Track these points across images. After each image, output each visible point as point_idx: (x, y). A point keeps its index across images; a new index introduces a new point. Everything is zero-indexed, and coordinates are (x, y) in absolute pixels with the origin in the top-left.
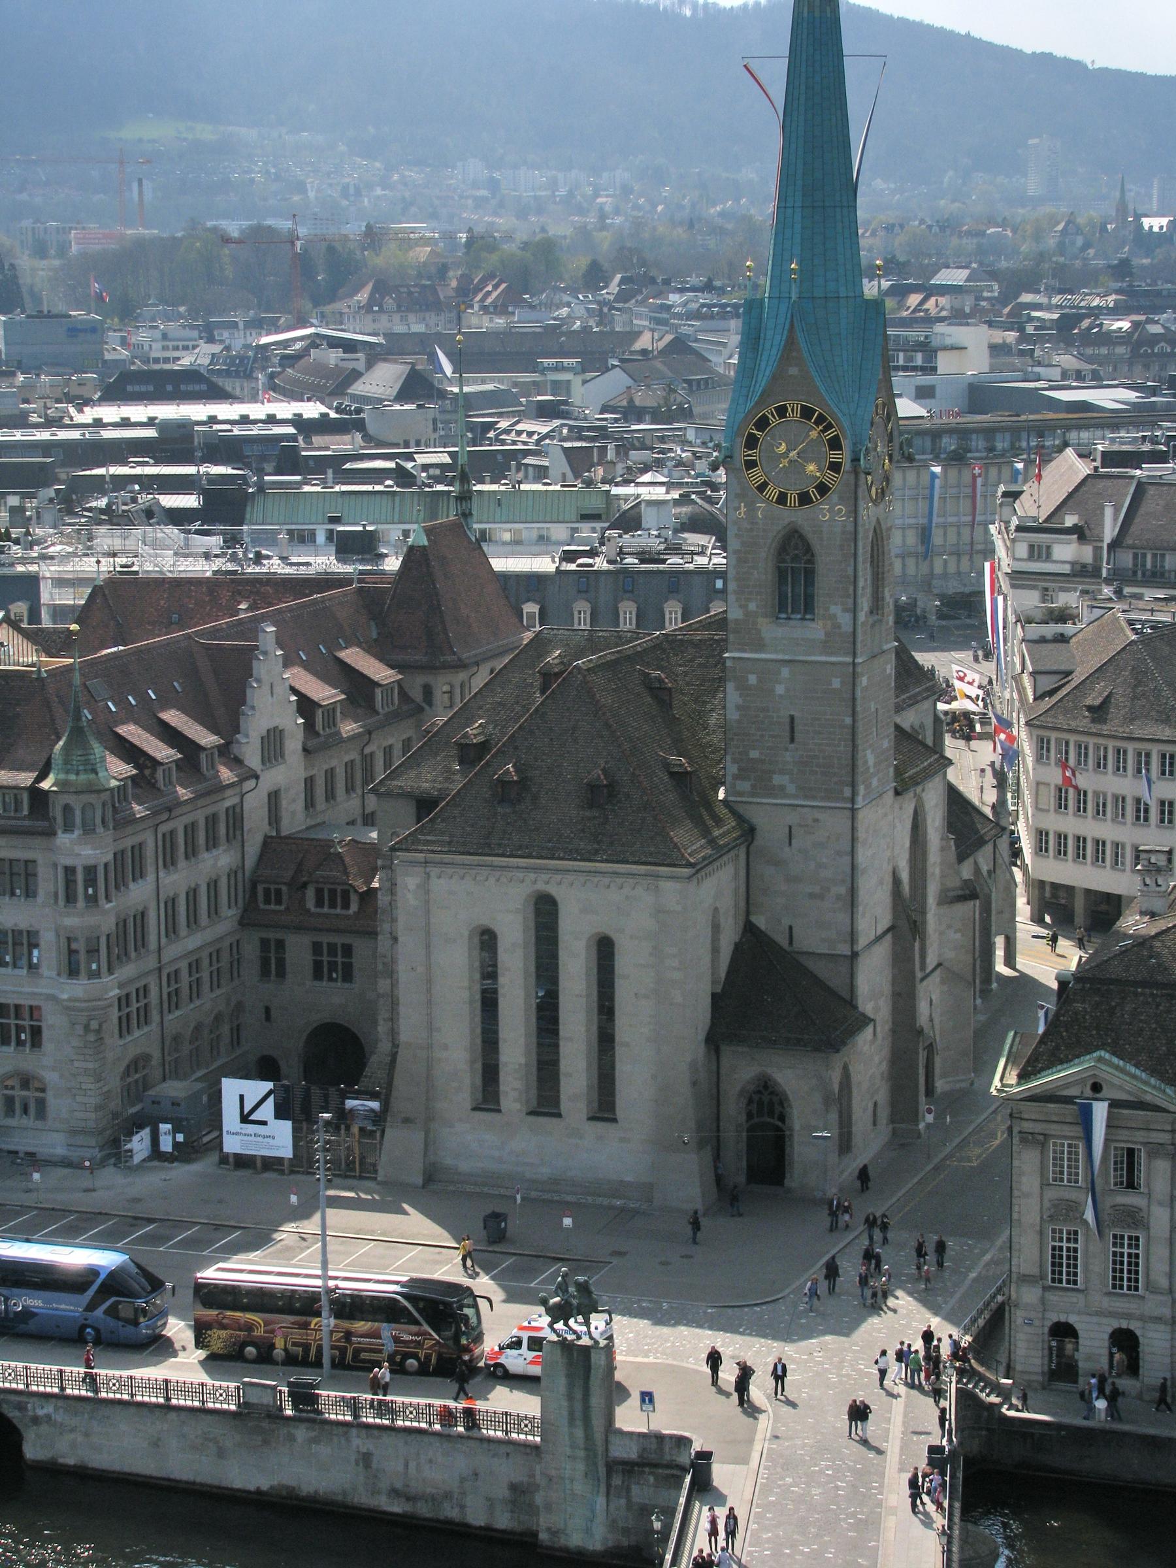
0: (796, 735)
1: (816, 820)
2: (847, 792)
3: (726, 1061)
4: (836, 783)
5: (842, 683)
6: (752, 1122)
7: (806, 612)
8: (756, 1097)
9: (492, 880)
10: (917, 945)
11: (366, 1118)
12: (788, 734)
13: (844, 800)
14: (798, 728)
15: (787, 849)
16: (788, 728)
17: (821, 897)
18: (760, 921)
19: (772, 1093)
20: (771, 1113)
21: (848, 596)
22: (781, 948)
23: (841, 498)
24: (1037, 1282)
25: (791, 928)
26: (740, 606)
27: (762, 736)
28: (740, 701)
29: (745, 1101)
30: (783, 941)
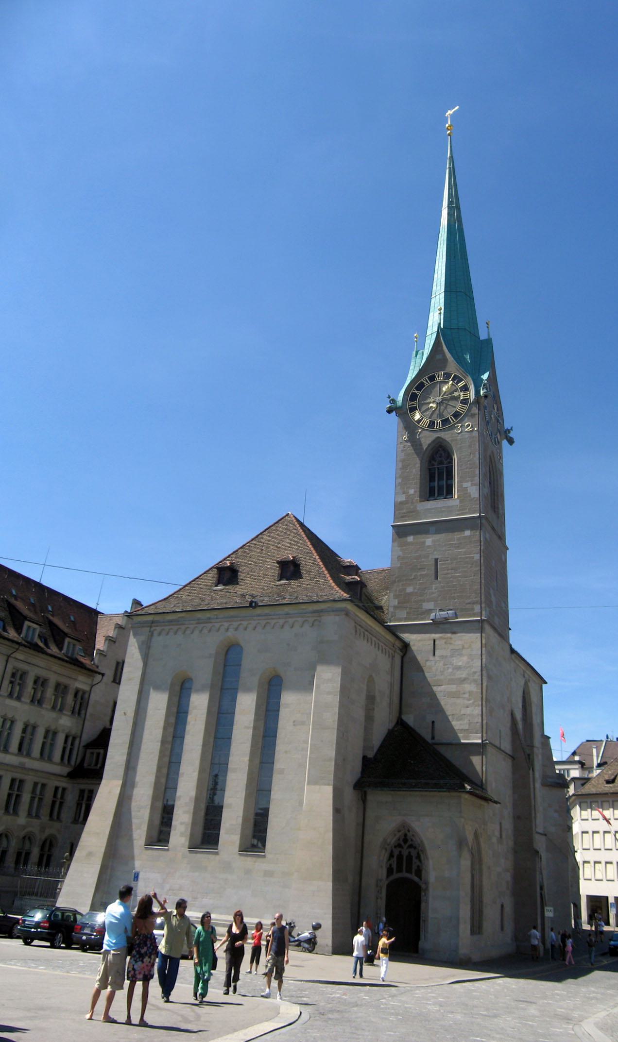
2: (477, 608)
3: (370, 813)
4: (469, 603)
6: (392, 878)
7: (446, 495)
8: (396, 853)
12: (433, 572)
13: (474, 615)
15: (432, 658)
16: (433, 568)
17: (455, 695)
18: (410, 719)
19: (411, 846)
20: (409, 870)
22: (424, 741)
25: (433, 722)
29: (387, 855)
30: (428, 737)
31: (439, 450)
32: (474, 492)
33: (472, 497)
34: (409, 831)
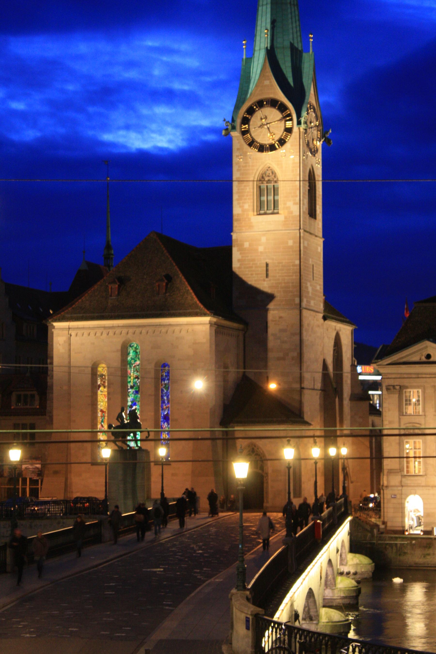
0: (270, 273)
1: (281, 317)
2: (297, 300)
5: (294, 243)
9: (105, 335)
10: (337, 400)
11: (33, 472)
12: (265, 272)
14: (270, 268)
16: (265, 269)
17: (283, 359)
21: (296, 196)
23: (292, 146)
24: (398, 472)
26: (240, 207)
27: (252, 274)
28: (240, 257)
31: (267, 170)
32: (295, 210)
33: (294, 214)
34: (255, 446)
